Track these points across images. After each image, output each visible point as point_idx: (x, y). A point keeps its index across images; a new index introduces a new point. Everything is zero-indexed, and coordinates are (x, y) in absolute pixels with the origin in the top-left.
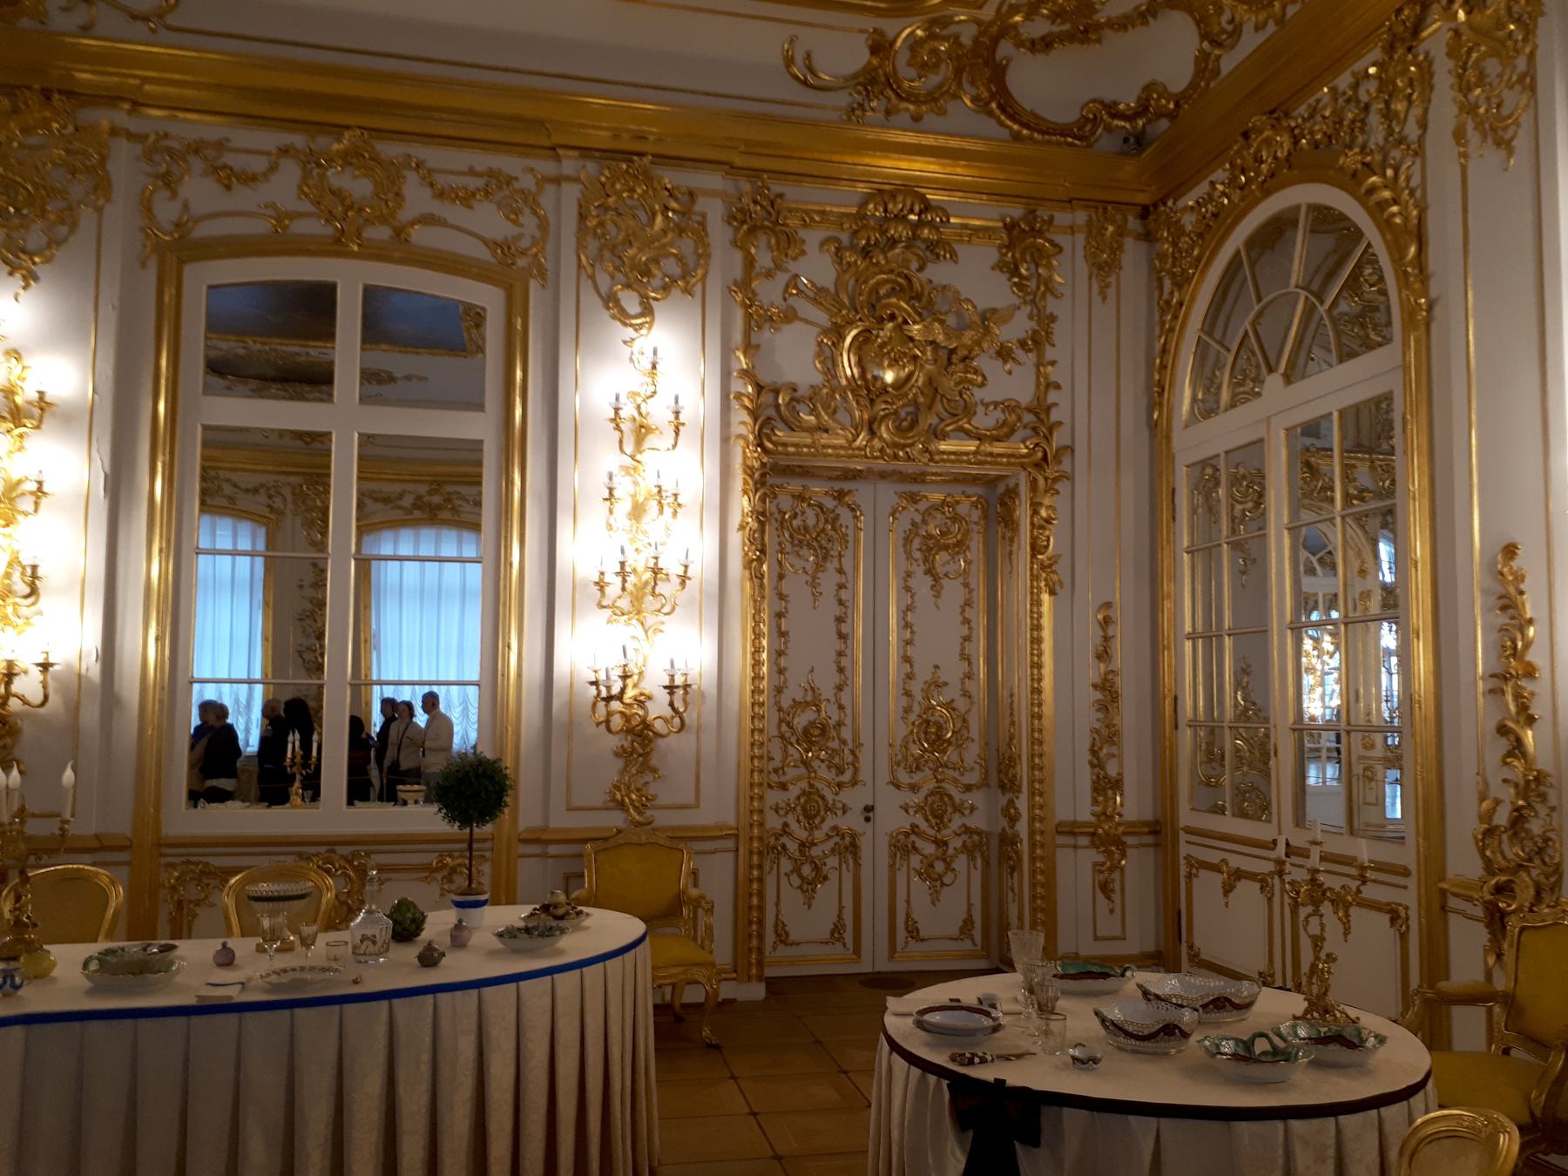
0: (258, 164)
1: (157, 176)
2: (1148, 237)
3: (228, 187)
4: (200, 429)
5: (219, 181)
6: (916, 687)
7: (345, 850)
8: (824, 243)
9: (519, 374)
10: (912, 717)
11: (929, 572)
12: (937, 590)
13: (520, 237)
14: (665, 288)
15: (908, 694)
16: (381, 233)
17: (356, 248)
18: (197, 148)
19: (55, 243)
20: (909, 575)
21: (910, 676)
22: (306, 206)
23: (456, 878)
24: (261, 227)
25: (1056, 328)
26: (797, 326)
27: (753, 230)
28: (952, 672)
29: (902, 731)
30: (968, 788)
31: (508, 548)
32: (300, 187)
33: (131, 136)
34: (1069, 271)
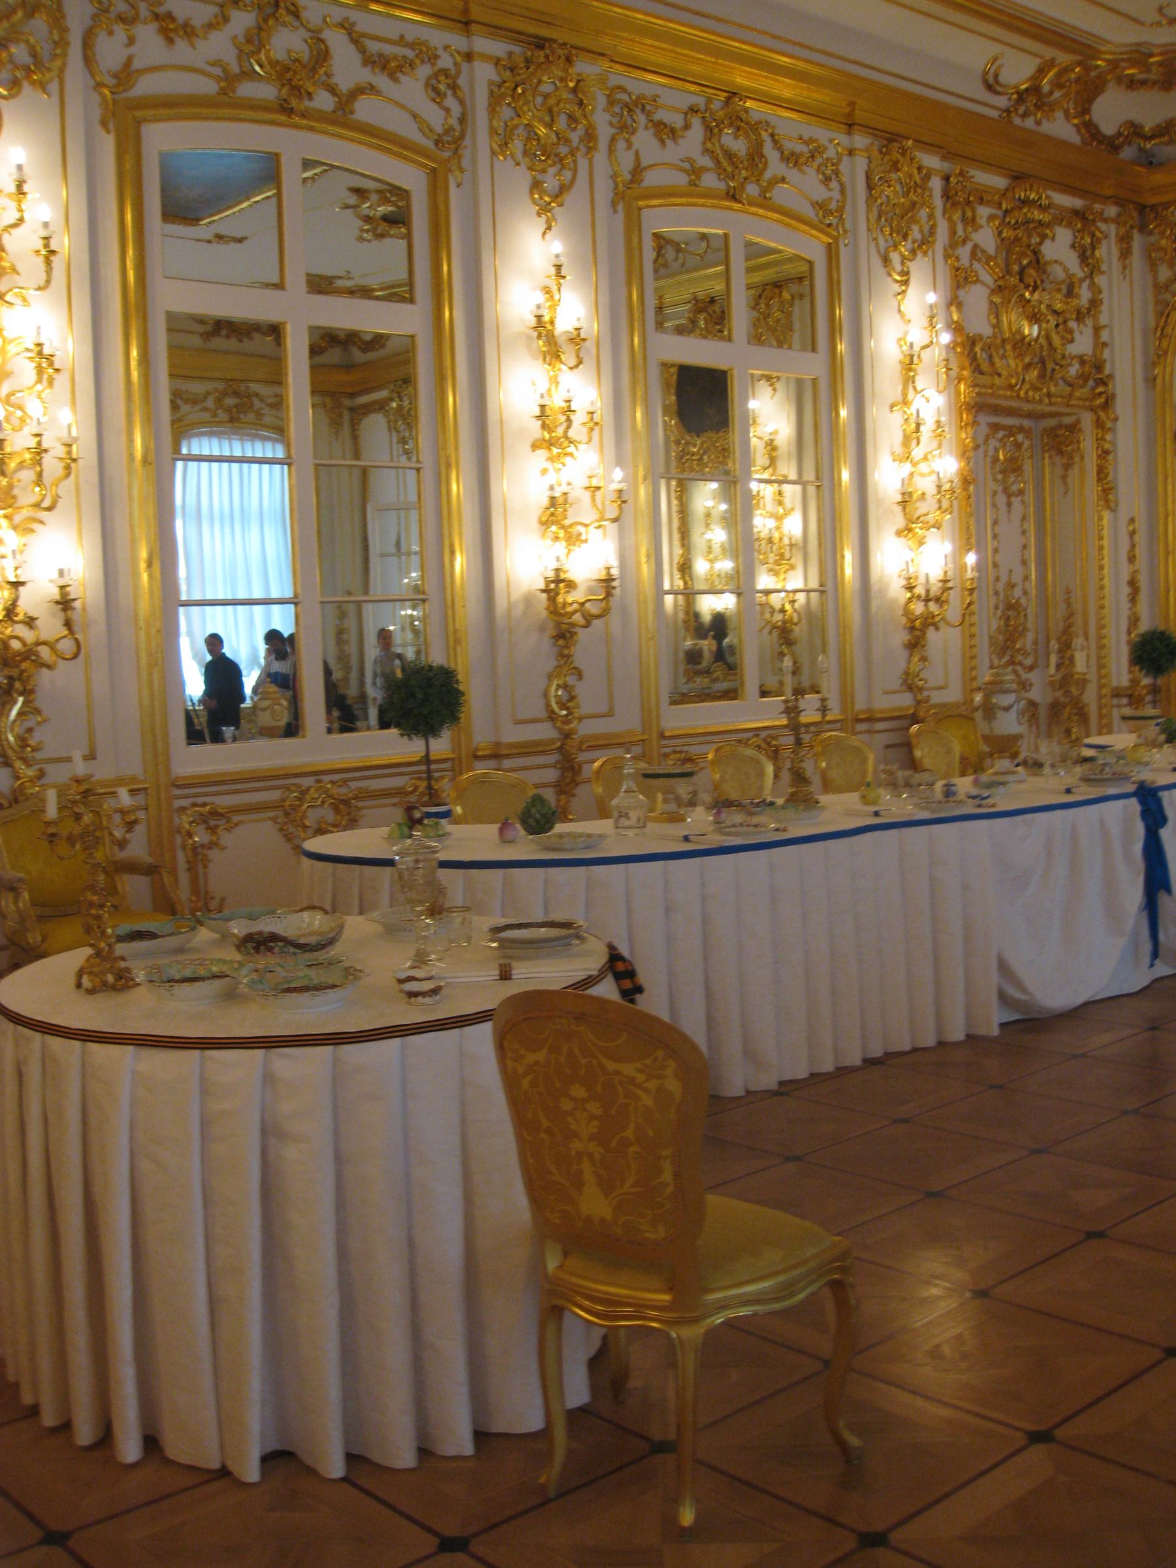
0: (677, 121)
2: (1142, 229)
6: (1000, 587)
7: (763, 734)
8: (991, 218)
10: (999, 613)
11: (1006, 491)
12: (1009, 505)
13: (831, 198)
14: (913, 252)
15: (996, 593)
20: (995, 493)
21: (997, 579)
25: (1104, 296)
26: (978, 286)
27: (954, 204)
28: (1017, 578)
29: (995, 624)
30: (1031, 668)
32: (704, 143)
34: (1108, 251)
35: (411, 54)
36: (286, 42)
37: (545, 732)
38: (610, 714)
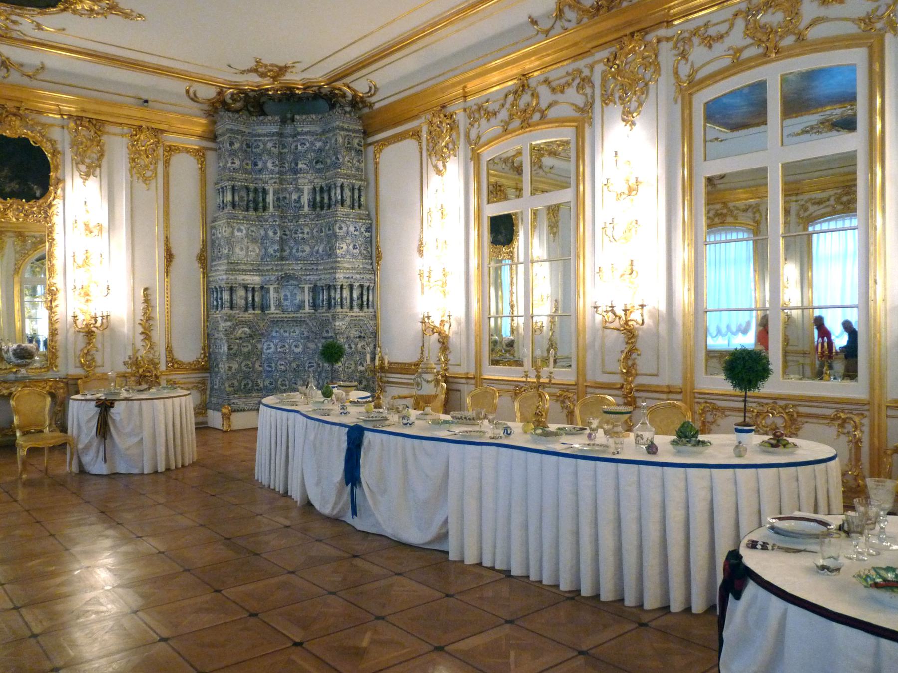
0: (723, 28)
1: (679, 55)
3: (710, 47)
4: (704, 181)
5: (706, 45)
7: (782, 403)
9: (878, 101)
13: (877, 9)
16: (789, 40)
17: (774, 55)
18: (695, 33)
19: (640, 104)
22: (749, 41)
23: (846, 425)
24: (727, 61)
31: (874, 217)
32: (744, 32)
33: (668, 39)
35: (569, 78)
36: (526, 98)
37: (617, 379)
38: (656, 375)
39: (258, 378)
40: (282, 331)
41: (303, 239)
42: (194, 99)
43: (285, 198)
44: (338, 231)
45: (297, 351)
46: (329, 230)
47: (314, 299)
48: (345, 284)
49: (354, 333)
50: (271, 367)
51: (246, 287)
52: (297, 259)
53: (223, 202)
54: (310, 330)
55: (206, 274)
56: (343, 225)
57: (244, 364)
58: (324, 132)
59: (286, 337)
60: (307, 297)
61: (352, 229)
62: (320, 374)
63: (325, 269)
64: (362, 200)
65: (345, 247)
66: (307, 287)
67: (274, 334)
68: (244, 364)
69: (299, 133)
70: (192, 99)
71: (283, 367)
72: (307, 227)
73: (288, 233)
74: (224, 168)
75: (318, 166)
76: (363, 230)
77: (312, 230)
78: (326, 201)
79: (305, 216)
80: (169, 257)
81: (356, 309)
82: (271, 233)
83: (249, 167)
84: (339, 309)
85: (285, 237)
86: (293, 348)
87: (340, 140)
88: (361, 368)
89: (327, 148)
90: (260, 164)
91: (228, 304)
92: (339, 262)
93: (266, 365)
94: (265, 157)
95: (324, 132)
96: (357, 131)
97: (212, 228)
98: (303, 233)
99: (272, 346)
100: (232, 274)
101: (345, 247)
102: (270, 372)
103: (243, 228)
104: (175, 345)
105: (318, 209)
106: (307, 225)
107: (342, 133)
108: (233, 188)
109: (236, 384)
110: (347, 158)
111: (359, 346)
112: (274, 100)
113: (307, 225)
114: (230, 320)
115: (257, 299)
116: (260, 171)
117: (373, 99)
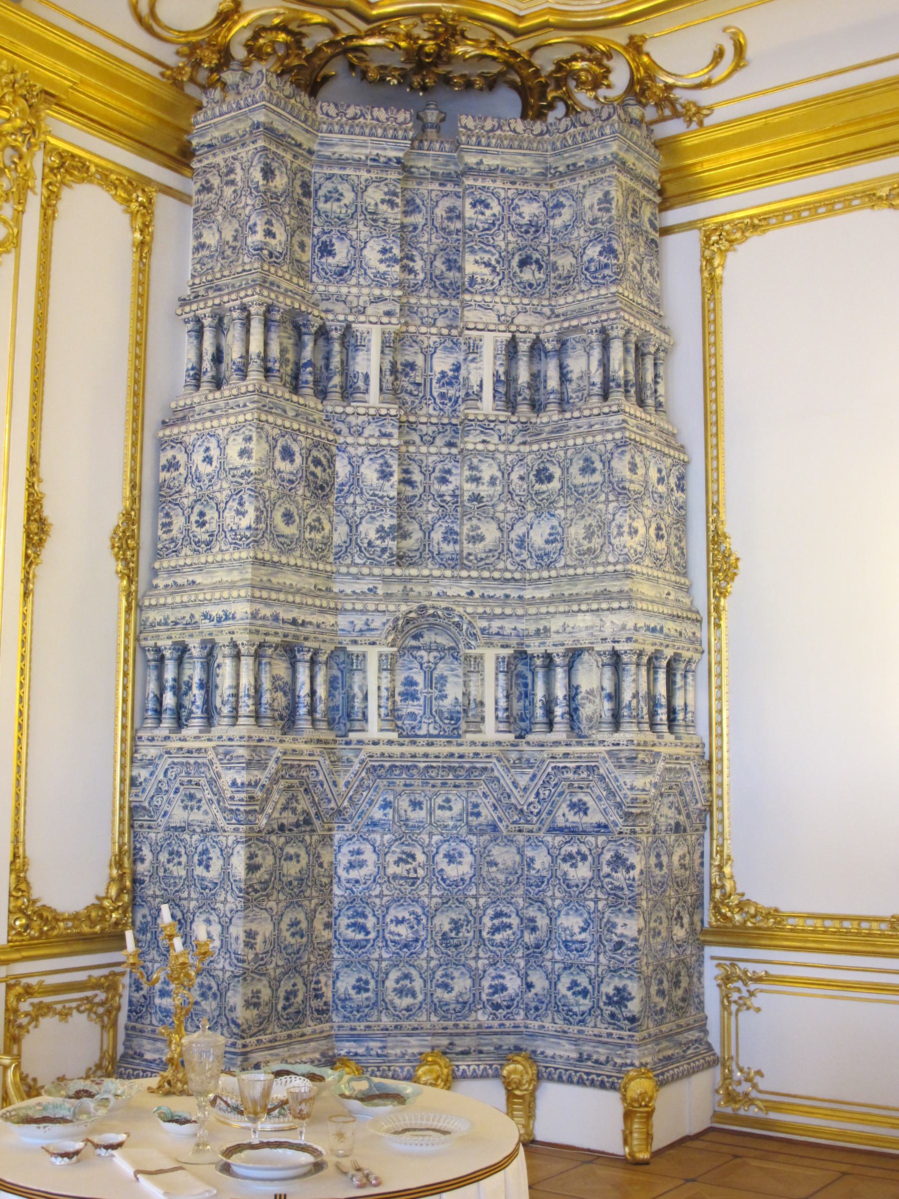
39: (320, 968)
40: (404, 804)
41: (476, 498)
42: (148, 22)
43: (412, 366)
44: (628, 475)
45: (453, 872)
46: (588, 469)
47: (507, 697)
48: (650, 649)
49: (666, 815)
50: (363, 928)
51: (290, 651)
52: (457, 562)
53: (218, 358)
54: (503, 801)
55: (134, 604)
56: (638, 460)
57: (286, 921)
58: (547, 174)
59: (420, 826)
60: (491, 689)
61: (654, 475)
62: (534, 952)
63: (552, 600)
64: (661, 389)
65: (642, 531)
66: (490, 656)
67: (377, 814)
68: (286, 921)
69: (468, 171)
70: (140, 20)
71: (403, 930)
72: (491, 463)
73: (417, 477)
74: (228, 252)
75: (527, 275)
76: (673, 481)
77: (506, 472)
78: (553, 383)
79: (486, 426)
80: (37, 530)
81: (669, 737)
82: (370, 473)
83: (306, 257)
84: (629, 733)
85: (409, 491)
86: (441, 862)
87: (616, 195)
88: (680, 933)
89: (557, 223)
90: (342, 253)
91: (246, 706)
92: (628, 575)
93: (343, 921)
94: (360, 230)
95: (547, 174)
96: (647, 183)
97: (177, 442)
98: (476, 480)
99: (369, 856)
100: (267, 602)
101: (639, 524)
102: (357, 945)
103: (296, 448)
104: (33, 850)
105: (524, 408)
106: (491, 455)
107: (623, 178)
108: (269, 309)
109: (266, 994)
110: (631, 257)
111: (675, 858)
112: (364, 75)
113: (491, 455)
114: (262, 765)
115: (321, 691)
116: (341, 273)
117: (704, 97)
